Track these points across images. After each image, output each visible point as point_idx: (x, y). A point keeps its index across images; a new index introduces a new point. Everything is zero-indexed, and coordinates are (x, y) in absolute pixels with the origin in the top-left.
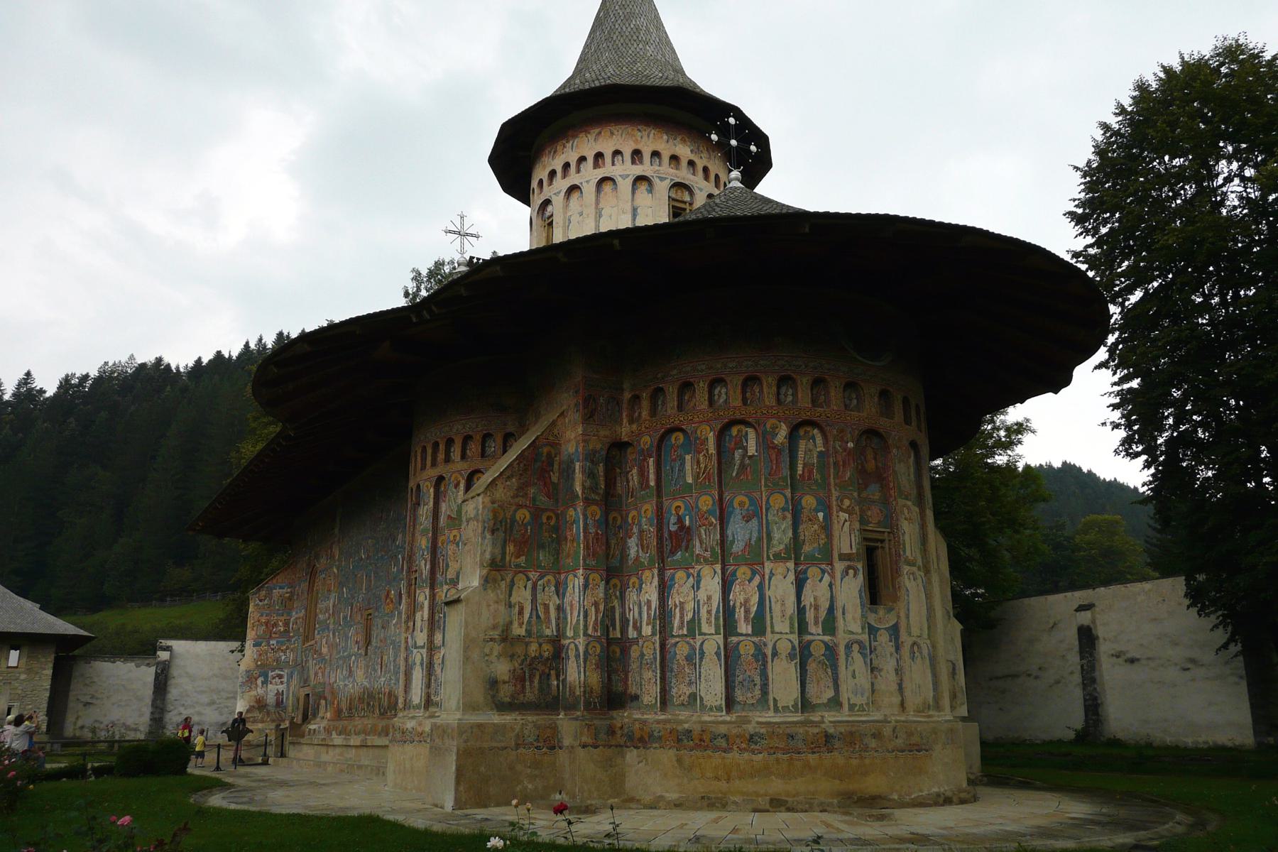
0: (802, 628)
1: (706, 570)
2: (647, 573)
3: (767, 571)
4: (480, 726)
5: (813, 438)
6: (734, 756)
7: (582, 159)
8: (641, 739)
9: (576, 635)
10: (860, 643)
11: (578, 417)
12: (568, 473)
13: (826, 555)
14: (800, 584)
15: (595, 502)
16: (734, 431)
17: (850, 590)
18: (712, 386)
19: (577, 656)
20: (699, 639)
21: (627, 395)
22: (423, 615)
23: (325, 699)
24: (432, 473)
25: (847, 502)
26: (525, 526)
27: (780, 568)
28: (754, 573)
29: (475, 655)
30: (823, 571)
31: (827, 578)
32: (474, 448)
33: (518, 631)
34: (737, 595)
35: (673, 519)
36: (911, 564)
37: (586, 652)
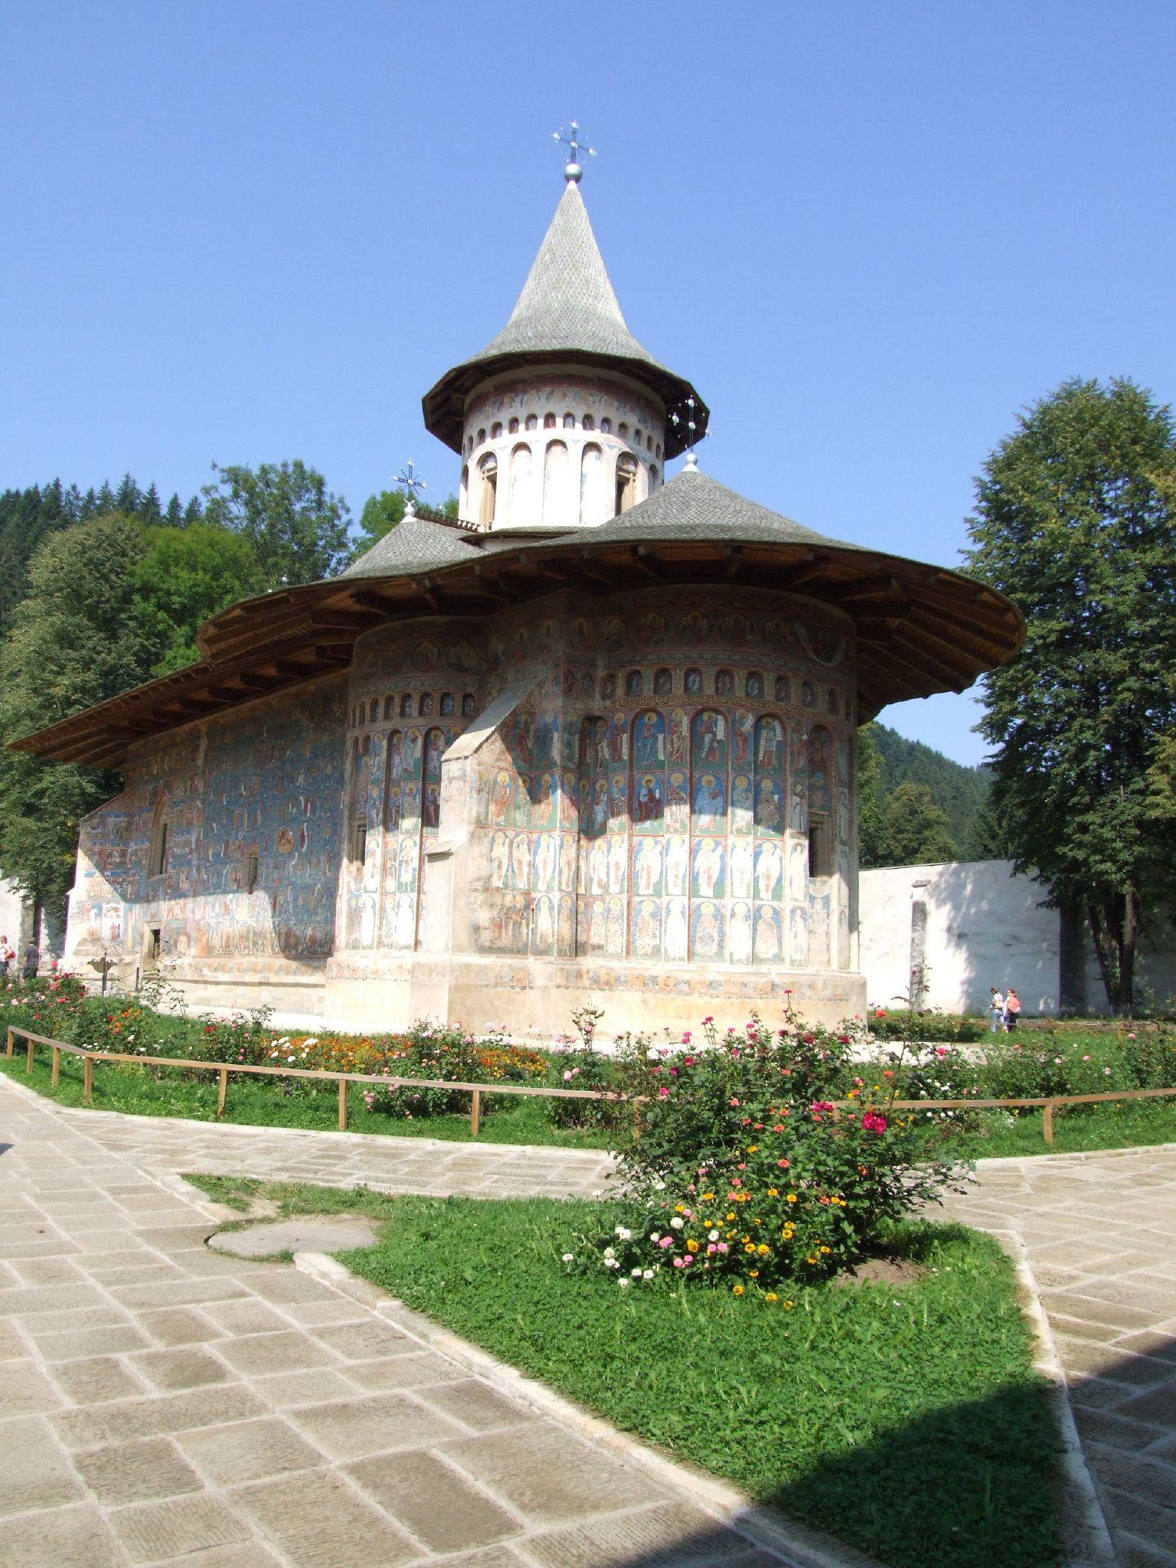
0: (756, 895)
1: (676, 840)
4: (467, 966)
5: (774, 729)
6: (695, 999)
8: (607, 983)
10: (802, 909)
11: (557, 690)
12: (544, 740)
14: (757, 855)
15: (571, 770)
16: (705, 716)
18: (687, 675)
19: (551, 908)
20: (665, 899)
21: (601, 673)
23: (189, 937)
24: (383, 725)
25: (799, 788)
26: (505, 787)
28: (717, 844)
30: (775, 846)
31: (778, 852)
32: (433, 705)
33: (497, 883)
34: (701, 862)
35: (644, 792)
36: (843, 843)
37: (560, 906)
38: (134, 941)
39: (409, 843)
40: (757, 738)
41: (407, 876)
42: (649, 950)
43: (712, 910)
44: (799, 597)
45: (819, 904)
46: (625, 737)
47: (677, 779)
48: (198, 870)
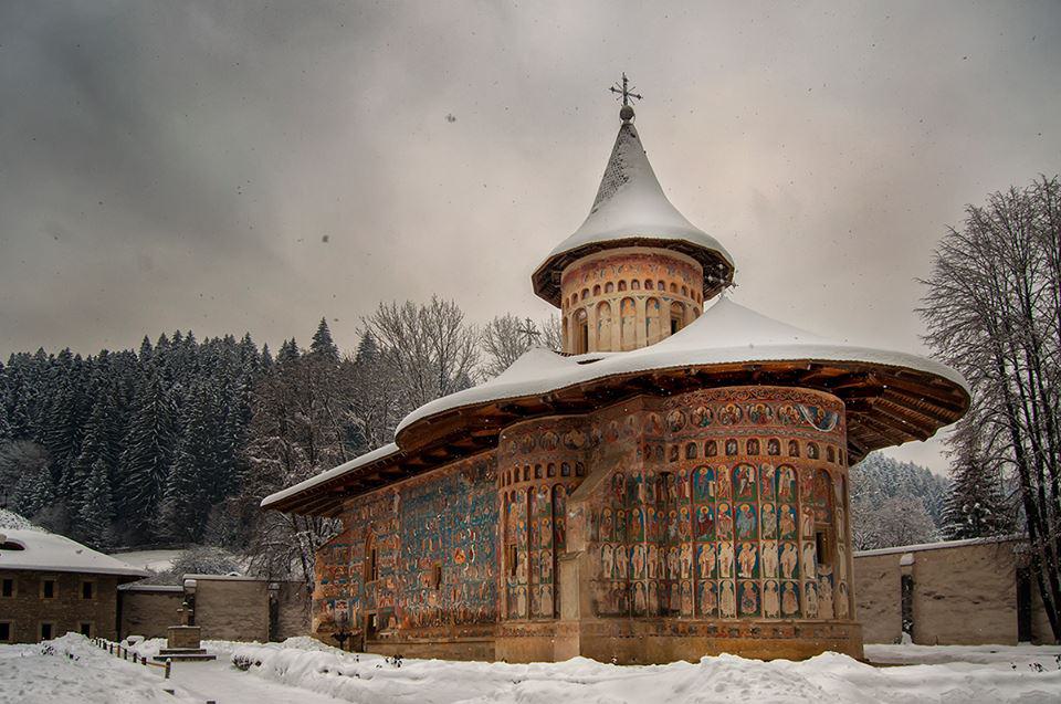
0: (782, 575)
1: (724, 546)
2: (684, 546)
3: (762, 545)
9: (642, 577)
19: (643, 588)
20: (720, 581)
22: (523, 566)
23: (394, 616)
27: (769, 544)
28: (753, 546)
29: (586, 588)
34: (743, 557)
37: (649, 587)
38: (357, 622)
39: (545, 554)
41: (546, 575)
42: (710, 611)
47: (723, 508)
48: (400, 577)
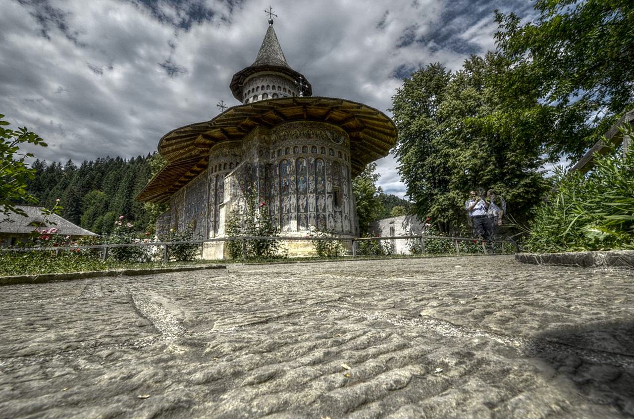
0: (317, 211)
1: (293, 196)
7: (258, 87)
12: (254, 171)
13: (324, 192)
14: (317, 199)
16: (300, 160)
17: (329, 202)
20: (290, 214)
24: (214, 174)
27: (312, 195)
32: (228, 166)
34: (300, 202)
36: (346, 196)
40: (316, 165)
42: (286, 229)
43: (304, 216)
44: (328, 124)
45: (338, 214)
46: (278, 168)
47: (292, 178)
